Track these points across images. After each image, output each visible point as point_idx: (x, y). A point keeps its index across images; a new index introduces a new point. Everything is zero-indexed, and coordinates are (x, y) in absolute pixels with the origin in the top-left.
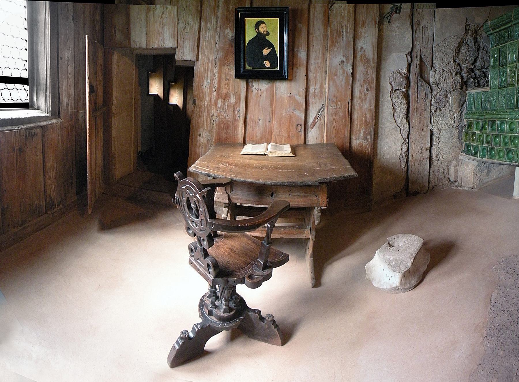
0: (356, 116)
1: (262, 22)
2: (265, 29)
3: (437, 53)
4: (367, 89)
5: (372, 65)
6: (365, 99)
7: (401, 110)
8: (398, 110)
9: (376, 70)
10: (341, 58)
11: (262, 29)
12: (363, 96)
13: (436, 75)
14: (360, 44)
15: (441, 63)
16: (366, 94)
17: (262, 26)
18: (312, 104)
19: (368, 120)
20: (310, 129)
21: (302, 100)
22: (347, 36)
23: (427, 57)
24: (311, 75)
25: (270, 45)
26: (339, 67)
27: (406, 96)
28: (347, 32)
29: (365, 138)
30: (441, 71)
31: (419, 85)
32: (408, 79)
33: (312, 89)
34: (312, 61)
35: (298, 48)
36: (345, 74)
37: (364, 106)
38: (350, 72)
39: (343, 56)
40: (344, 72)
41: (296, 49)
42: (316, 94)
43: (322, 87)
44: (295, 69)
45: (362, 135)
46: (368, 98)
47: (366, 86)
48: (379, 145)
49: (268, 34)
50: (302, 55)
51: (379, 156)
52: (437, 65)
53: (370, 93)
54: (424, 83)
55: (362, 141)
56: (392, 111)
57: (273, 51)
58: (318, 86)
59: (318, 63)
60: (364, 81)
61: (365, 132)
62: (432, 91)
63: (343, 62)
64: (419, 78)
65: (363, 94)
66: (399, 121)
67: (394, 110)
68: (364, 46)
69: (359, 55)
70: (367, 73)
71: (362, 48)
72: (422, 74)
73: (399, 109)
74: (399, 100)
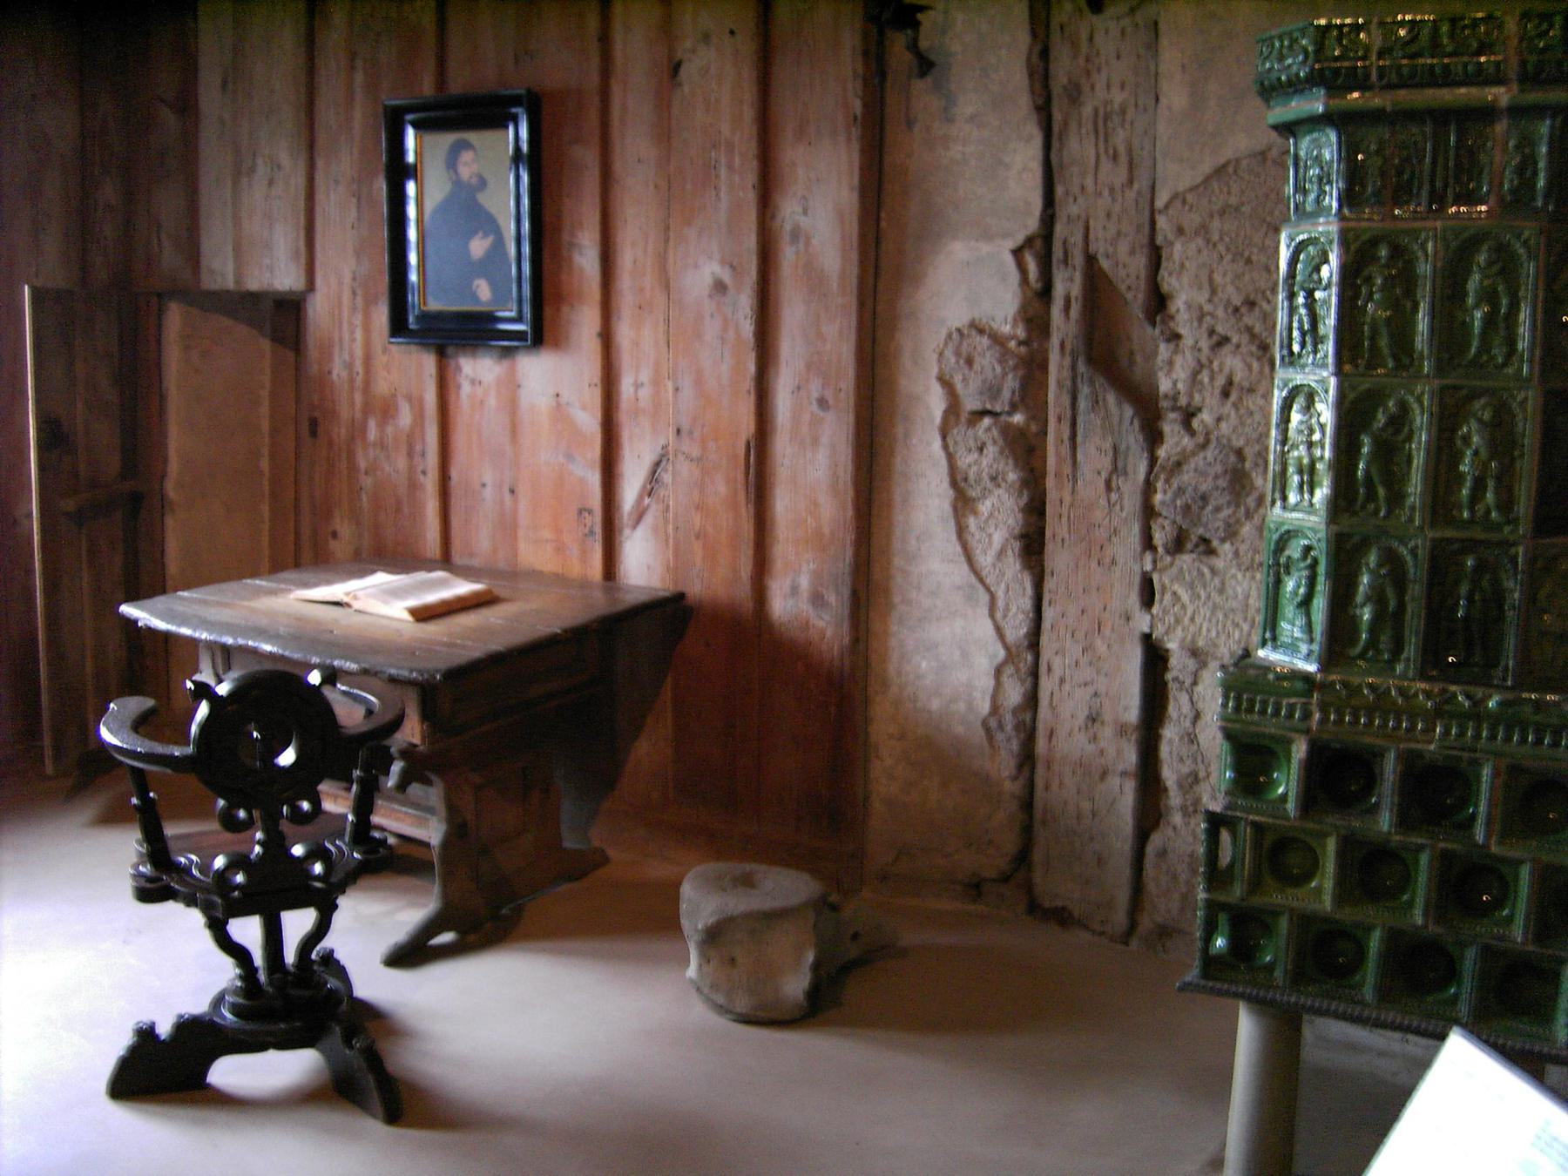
0: (783, 504)
1: (467, 145)
2: (475, 168)
3: (1178, 247)
4: (822, 403)
5: (840, 300)
6: (815, 441)
7: (1000, 513)
8: (985, 507)
9: (854, 323)
10: (711, 269)
11: (468, 166)
12: (805, 430)
13: (1179, 360)
14: (789, 211)
15: (1202, 297)
16: (816, 422)
17: (467, 156)
18: (631, 438)
19: (826, 530)
20: (627, 532)
21: (589, 421)
22: (735, 186)
23: (1127, 269)
24: (624, 333)
25: (488, 224)
26: (709, 306)
27: (1026, 450)
28: (730, 167)
29: (817, 599)
30: (1205, 344)
31: (1083, 404)
32: (1033, 368)
33: (626, 387)
34: (625, 283)
35: (573, 235)
36: (731, 334)
37: (812, 472)
38: (748, 328)
39: (723, 262)
40: (725, 329)
41: (566, 237)
42: (642, 404)
43: (657, 383)
44: (565, 309)
45: (804, 582)
46: (825, 440)
47: (815, 389)
48: (893, 642)
49: (483, 183)
50: (587, 261)
51: (894, 690)
52: (1182, 307)
53: (830, 417)
54: (1111, 398)
55: (804, 606)
56: (946, 506)
57: (499, 242)
58: (645, 376)
59: (642, 290)
60: (808, 367)
61: (817, 576)
62: (1153, 437)
63: (720, 287)
64: (1082, 367)
65: (806, 417)
66: (985, 560)
67: (963, 503)
68: (804, 222)
69: (788, 256)
70: (820, 336)
71: (796, 234)
72: (1107, 358)
73: (988, 503)
74: (986, 458)
